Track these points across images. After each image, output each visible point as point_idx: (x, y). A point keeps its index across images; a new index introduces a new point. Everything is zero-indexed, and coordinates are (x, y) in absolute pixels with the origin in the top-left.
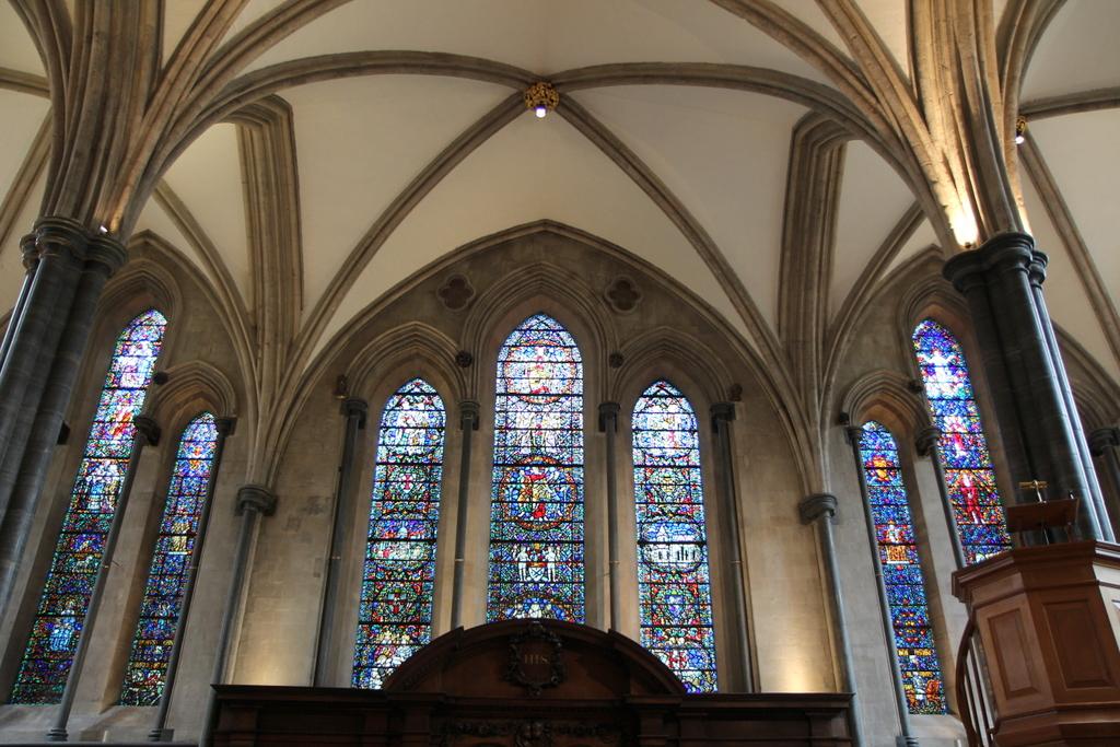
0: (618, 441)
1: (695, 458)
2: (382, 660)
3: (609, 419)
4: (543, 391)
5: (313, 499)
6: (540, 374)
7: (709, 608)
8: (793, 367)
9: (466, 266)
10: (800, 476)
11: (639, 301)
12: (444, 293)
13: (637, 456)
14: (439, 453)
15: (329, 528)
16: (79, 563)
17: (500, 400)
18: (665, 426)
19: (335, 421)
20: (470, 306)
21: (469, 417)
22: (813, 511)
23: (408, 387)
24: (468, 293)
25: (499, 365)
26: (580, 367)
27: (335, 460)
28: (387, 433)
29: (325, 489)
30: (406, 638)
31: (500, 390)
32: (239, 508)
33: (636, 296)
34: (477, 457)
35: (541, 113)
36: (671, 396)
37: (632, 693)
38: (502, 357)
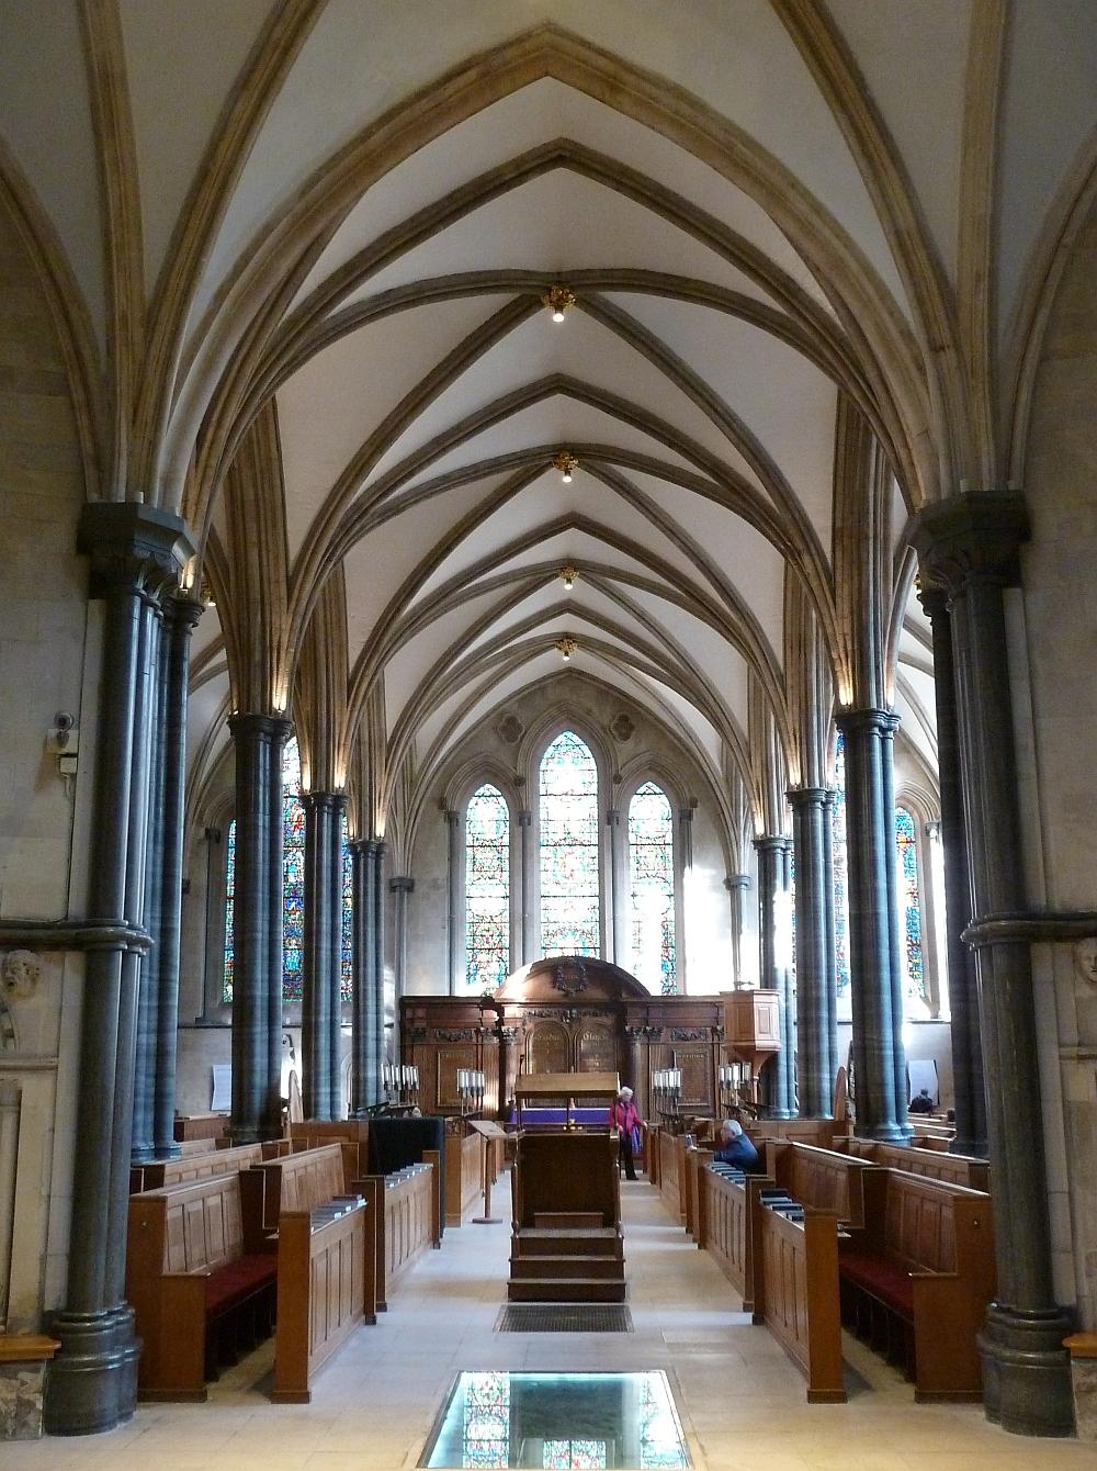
0: (618, 830)
1: (669, 839)
2: (481, 972)
3: (612, 818)
4: (570, 793)
5: (435, 881)
6: (567, 773)
7: (673, 936)
8: (729, 789)
9: (517, 705)
10: (730, 861)
11: (634, 733)
12: (504, 729)
13: (632, 838)
14: (506, 840)
15: (447, 897)
16: (292, 916)
17: (542, 799)
18: (650, 811)
19: (443, 827)
20: (521, 741)
21: (522, 819)
22: (732, 884)
23: (481, 791)
24: (520, 729)
25: (541, 773)
26: (595, 773)
27: (446, 855)
28: (472, 825)
29: (441, 873)
30: (495, 958)
31: (542, 792)
32: (393, 889)
33: (632, 728)
34: (531, 844)
35: (559, 318)
36: (655, 794)
37: (624, 995)
38: (542, 767)
